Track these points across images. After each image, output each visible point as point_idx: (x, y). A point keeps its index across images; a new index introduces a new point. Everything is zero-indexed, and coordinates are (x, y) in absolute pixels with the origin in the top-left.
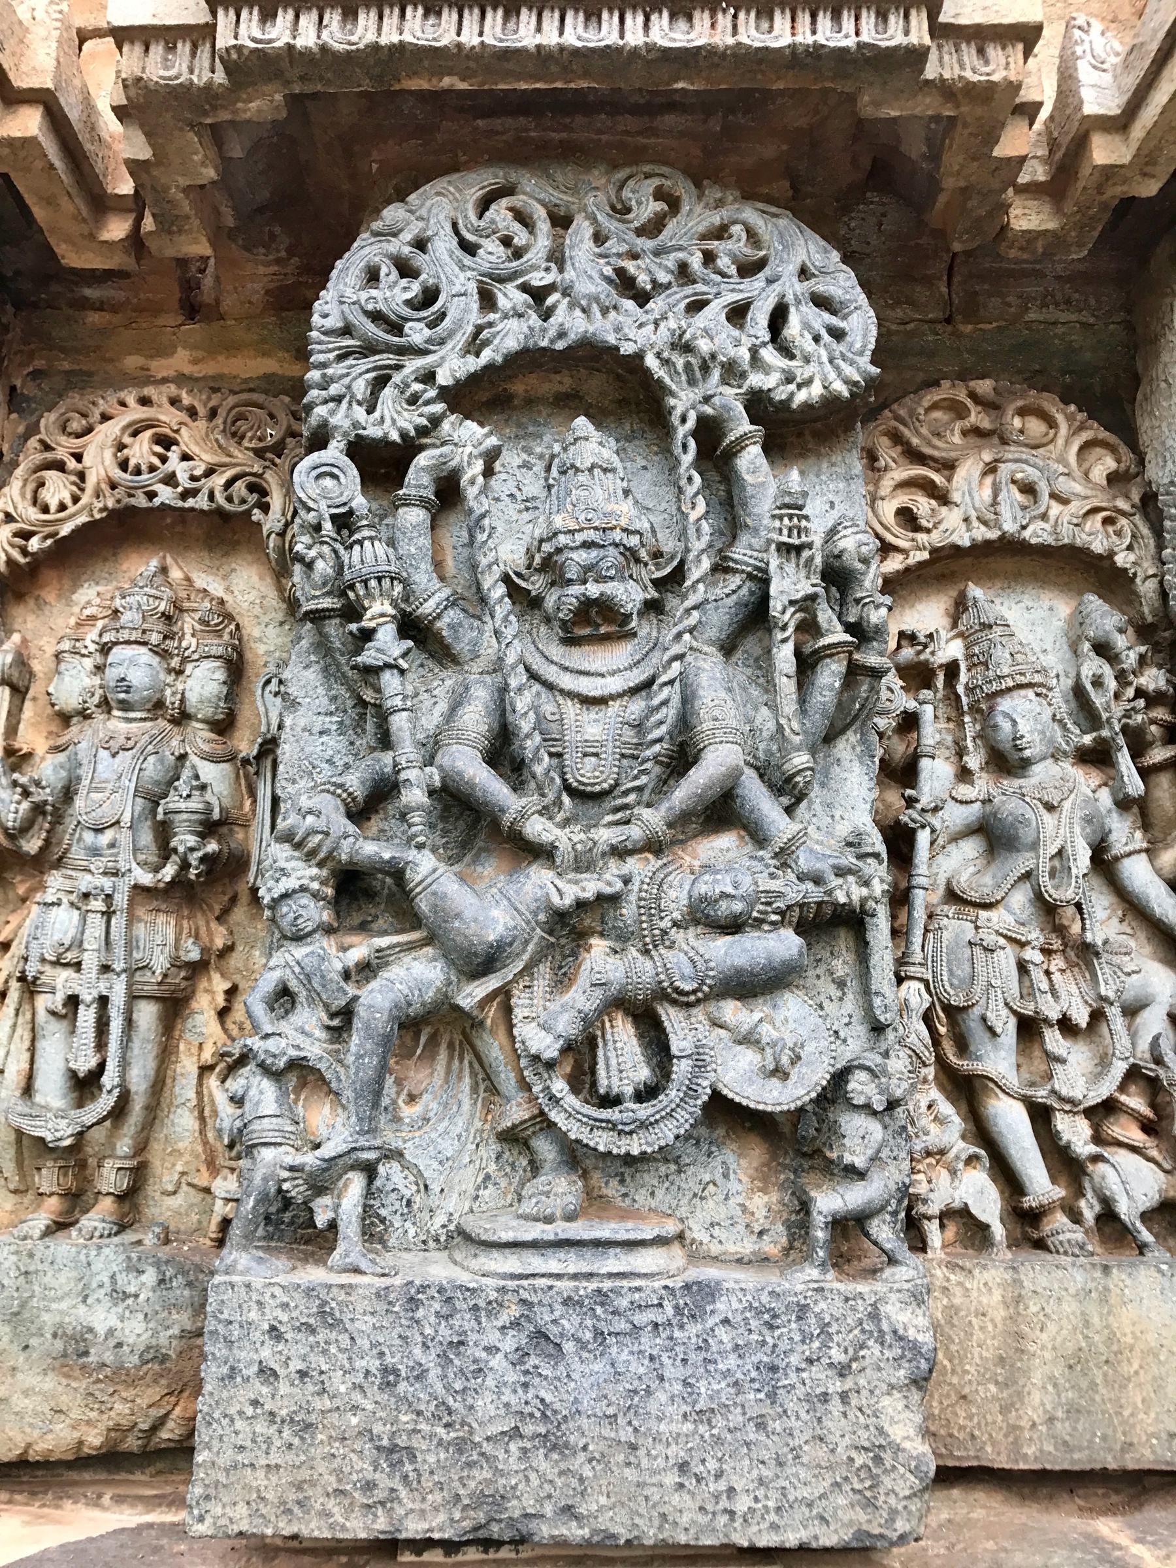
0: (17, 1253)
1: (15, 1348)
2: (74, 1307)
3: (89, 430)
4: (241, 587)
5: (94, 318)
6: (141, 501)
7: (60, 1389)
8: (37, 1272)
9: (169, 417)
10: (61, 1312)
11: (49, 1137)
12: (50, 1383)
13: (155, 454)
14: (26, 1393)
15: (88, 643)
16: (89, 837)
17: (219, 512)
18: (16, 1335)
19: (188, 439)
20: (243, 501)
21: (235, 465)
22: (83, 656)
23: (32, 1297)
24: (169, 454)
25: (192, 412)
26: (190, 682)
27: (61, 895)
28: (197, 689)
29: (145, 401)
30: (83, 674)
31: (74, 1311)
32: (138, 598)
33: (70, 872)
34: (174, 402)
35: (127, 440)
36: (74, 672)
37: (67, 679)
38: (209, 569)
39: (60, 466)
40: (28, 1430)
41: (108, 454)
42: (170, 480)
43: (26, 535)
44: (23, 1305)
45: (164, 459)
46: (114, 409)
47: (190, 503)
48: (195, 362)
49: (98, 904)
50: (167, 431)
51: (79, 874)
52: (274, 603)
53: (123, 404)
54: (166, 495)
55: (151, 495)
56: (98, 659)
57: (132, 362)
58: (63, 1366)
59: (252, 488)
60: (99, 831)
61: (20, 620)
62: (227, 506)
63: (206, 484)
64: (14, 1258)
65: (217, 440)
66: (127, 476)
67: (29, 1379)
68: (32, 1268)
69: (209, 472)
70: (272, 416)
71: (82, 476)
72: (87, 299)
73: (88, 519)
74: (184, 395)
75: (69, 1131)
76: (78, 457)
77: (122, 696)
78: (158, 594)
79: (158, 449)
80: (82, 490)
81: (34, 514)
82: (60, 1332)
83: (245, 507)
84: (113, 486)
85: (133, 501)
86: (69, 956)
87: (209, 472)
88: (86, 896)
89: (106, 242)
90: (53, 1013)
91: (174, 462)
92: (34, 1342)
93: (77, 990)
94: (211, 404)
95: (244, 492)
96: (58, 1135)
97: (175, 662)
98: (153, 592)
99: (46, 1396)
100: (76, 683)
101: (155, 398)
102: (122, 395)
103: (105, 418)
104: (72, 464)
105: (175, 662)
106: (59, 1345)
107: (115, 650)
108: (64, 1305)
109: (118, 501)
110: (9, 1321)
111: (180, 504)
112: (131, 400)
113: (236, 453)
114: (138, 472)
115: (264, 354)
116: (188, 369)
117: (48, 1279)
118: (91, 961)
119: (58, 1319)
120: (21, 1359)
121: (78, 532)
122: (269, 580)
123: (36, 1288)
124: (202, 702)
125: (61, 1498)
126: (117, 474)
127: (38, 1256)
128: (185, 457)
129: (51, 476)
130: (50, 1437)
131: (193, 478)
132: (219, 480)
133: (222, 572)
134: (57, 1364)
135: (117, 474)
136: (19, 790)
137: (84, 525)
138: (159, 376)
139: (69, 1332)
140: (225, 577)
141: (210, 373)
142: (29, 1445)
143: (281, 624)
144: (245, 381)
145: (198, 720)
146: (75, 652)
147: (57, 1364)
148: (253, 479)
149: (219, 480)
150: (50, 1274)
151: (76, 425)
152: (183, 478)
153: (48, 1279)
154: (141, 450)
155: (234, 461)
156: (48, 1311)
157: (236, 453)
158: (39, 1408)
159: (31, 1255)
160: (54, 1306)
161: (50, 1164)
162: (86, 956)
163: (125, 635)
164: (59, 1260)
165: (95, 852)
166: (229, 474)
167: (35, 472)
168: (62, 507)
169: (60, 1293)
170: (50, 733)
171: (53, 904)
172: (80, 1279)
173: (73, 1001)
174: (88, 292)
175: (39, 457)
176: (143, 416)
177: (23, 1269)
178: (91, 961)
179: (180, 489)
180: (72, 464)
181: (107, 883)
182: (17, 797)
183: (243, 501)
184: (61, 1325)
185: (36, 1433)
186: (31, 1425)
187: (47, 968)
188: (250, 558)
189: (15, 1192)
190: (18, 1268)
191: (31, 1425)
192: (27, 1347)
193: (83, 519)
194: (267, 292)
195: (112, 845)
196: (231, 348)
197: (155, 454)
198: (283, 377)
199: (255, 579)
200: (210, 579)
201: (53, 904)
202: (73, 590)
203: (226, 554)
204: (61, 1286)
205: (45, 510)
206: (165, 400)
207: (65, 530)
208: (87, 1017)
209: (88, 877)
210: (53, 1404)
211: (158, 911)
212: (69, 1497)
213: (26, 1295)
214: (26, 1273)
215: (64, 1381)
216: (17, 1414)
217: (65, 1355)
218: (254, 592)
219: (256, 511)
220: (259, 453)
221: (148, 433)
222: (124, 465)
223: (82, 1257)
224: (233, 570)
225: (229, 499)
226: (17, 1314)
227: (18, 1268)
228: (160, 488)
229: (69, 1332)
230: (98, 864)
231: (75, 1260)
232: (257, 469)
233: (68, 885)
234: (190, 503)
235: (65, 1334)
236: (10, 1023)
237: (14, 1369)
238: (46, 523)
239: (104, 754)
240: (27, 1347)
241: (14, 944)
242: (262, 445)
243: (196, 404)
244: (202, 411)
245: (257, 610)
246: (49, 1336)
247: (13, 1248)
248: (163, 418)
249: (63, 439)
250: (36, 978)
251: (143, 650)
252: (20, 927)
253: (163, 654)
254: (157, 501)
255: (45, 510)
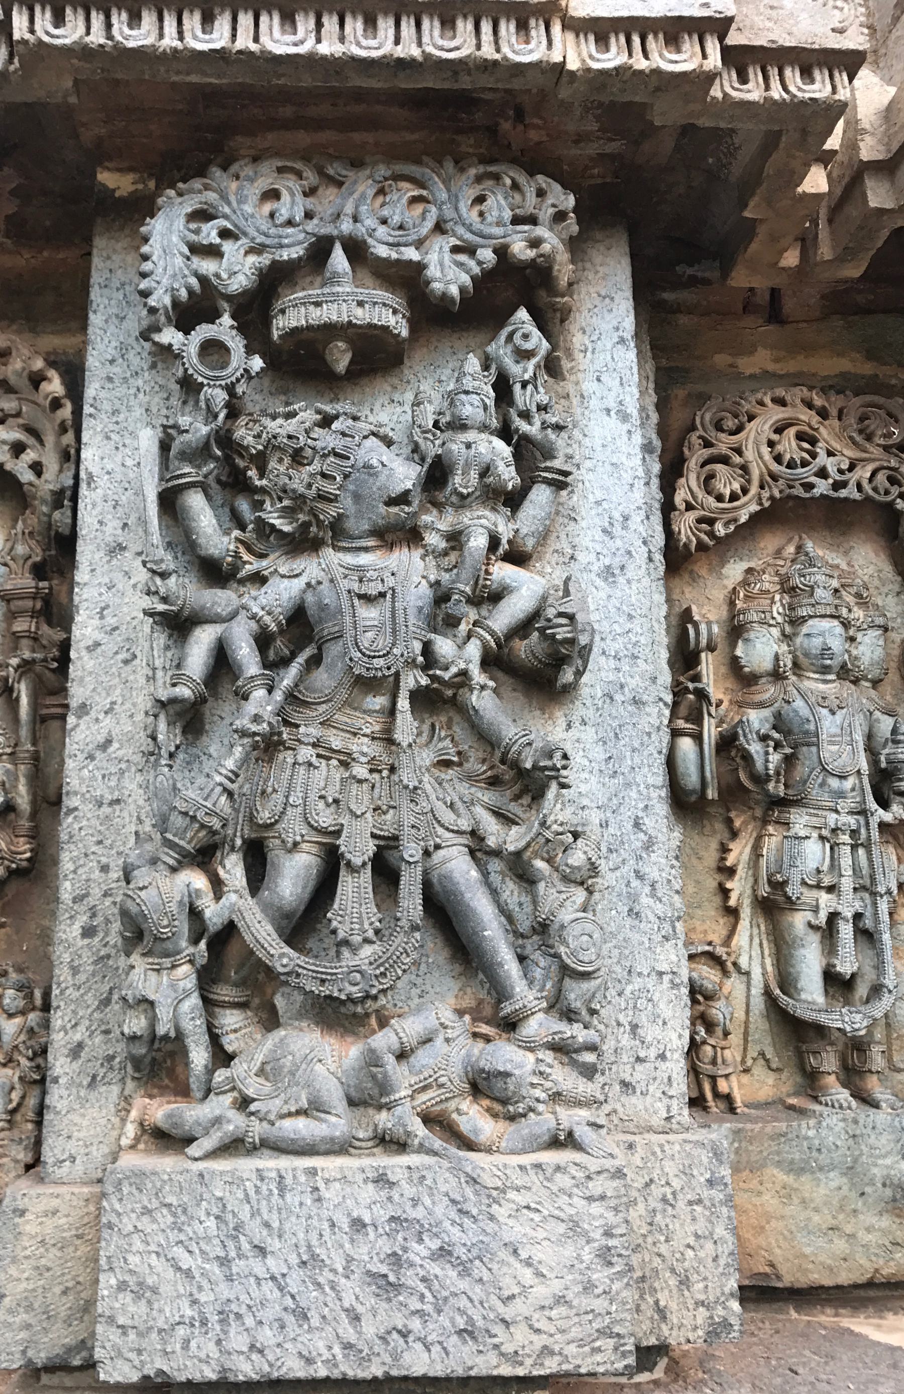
0: (844, 1120)
1: (854, 1195)
2: (897, 1162)
3: (739, 429)
4: (861, 562)
5: (683, 320)
6: (799, 491)
7: (894, 1226)
8: (862, 1135)
9: (805, 415)
10: (887, 1167)
11: (848, 1029)
12: (885, 1222)
13: (802, 449)
14: (868, 1230)
15: (775, 615)
16: (834, 783)
17: (868, 499)
18: (853, 1185)
19: (826, 434)
20: (887, 493)
21: (874, 460)
22: (771, 625)
23: (861, 1154)
24: (818, 450)
25: (823, 414)
26: (861, 648)
27: (809, 830)
28: (868, 654)
29: (781, 402)
30: (772, 641)
31: (897, 1166)
32: (818, 577)
33: (812, 811)
34: (810, 405)
35: (775, 437)
36: (764, 639)
37: (758, 646)
38: (831, 547)
39: (724, 460)
40: (874, 1259)
41: (765, 450)
42: (822, 473)
43: (711, 522)
44: (855, 1161)
45: (814, 455)
46: (758, 409)
47: (843, 493)
48: (777, 360)
49: (846, 838)
50: (807, 428)
51: (825, 813)
52: (890, 576)
53: (761, 403)
54: (822, 487)
55: (809, 487)
56: (788, 629)
57: (721, 360)
58: (895, 1209)
59: (892, 480)
60: (843, 777)
61: (677, 591)
62: (876, 496)
63: (853, 477)
64: (842, 1124)
65: (851, 438)
66: (783, 469)
67: (869, 1218)
68: (858, 1132)
69: (851, 468)
70: (890, 415)
71: (745, 468)
72: (665, 301)
73: (758, 508)
74: (815, 397)
75: (865, 1024)
76: (739, 451)
77: (828, 662)
78: (831, 573)
79: (806, 445)
80: (749, 481)
81: (711, 501)
82: (888, 1182)
83: (889, 498)
84: (774, 477)
85: (795, 492)
86: (827, 881)
87: (851, 468)
88: (834, 831)
89: (783, 268)
90: (810, 925)
91: (822, 459)
92: (868, 1190)
93: (840, 909)
94: (839, 404)
95: (887, 485)
96: (856, 1026)
97: (851, 632)
98: (828, 572)
99: (884, 1232)
100: (767, 649)
101: (788, 398)
102: (759, 396)
103: (751, 418)
104: (737, 459)
105: (851, 632)
106: (888, 1192)
107: (810, 622)
108: (888, 1161)
109: (781, 492)
110: (845, 1174)
111: (835, 495)
112: (767, 400)
113: (872, 449)
114: (791, 465)
115: (840, 355)
116: (771, 367)
117: (872, 1140)
118: (847, 884)
119: (885, 1173)
120: (860, 1204)
121: (754, 517)
122: (883, 556)
123: (863, 1147)
124: (872, 665)
125: (882, 1311)
126: (774, 467)
127: (861, 1122)
128: (830, 454)
129: (719, 467)
130: (892, 1263)
131: (841, 471)
132: (864, 473)
133: (842, 549)
134: (889, 1207)
135: (774, 467)
136: (772, 743)
137: (757, 513)
138: (748, 373)
139: (896, 1181)
140: (846, 553)
141: (791, 371)
142: (877, 1271)
143: (898, 594)
144: (825, 378)
145: (867, 680)
146: (762, 623)
147: (889, 1207)
148: (891, 473)
149: (864, 473)
150: (873, 1137)
151: (730, 423)
152: (832, 470)
153: (872, 1140)
154: (789, 446)
155: (873, 456)
156: (876, 1165)
157: (872, 449)
158: (880, 1242)
159: (856, 1122)
160: (880, 1162)
161: (829, 1048)
162: (843, 880)
163: (821, 610)
164: (878, 1126)
165: (840, 794)
166: (870, 468)
167: (702, 466)
168: (734, 497)
169: (883, 1151)
170: (727, 689)
171: (807, 837)
172: (898, 1141)
173: (833, 917)
174: (668, 296)
175: (706, 453)
176: (786, 415)
177: (851, 1133)
178: (847, 884)
179: (831, 481)
180: (737, 459)
181: (852, 821)
182: (771, 750)
183: (887, 493)
184: (888, 1176)
185: (881, 1262)
186: (876, 1255)
187: (804, 890)
188: (863, 536)
189: (778, 1070)
190: (847, 1132)
191: (876, 1255)
192: (863, 1194)
193: (754, 508)
194: (823, 297)
195: (853, 790)
196: (808, 349)
197: (802, 449)
198: (856, 375)
199: (872, 555)
200: (834, 555)
201: (807, 837)
202: (723, 564)
203: (844, 534)
204: (883, 1145)
205: (720, 498)
206: (798, 401)
207: (743, 519)
208: (846, 931)
209: (834, 816)
210: (891, 1238)
211: (887, 842)
212: (889, 1310)
213: (857, 1153)
214: (854, 1136)
215: (898, 1221)
216: (863, 1246)
217: (894, 1200)
218: (872, 567)
219: (898, 500)
220: (886, 448)
221: (792, 432)
222: (778, 459)
223: (897, 1123)
224: (852, 547)
225: (875, 489)
226: (852, 1168)
227: (847, 1132)
228: (813, 479)
229: (896, 1181)
230: (843, 805)
231: (890, 1126)
232: (893, 463)
233: (815, 821)
234: (843, 493)
235: (892, 1183)
236: (748, 934)
237: (855, 1211)
238: (724, 511)
239: (825, 712)
240: (863, 1194)
241: (740, 867)
242: (891, 442)
243: (827, 405)
244: (834, 412)
245: (876, 582)
246: (879, 1185)
247: (840, 1116)
248: (803, 417)
249: (722, 436)
250: (798, 898)
251: (836, 623)
252: (741, 854)
253: (846, 625)
254: (817, 492)
255: (720, 498)
